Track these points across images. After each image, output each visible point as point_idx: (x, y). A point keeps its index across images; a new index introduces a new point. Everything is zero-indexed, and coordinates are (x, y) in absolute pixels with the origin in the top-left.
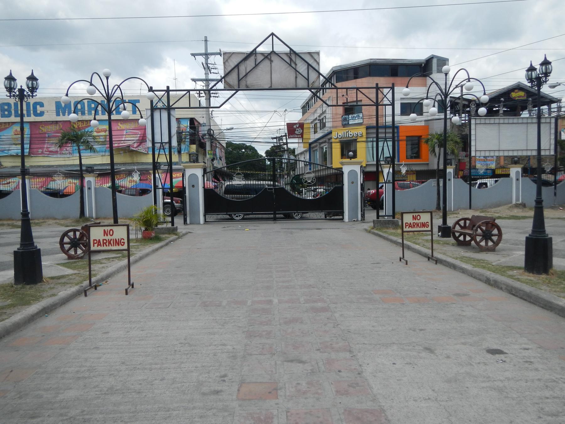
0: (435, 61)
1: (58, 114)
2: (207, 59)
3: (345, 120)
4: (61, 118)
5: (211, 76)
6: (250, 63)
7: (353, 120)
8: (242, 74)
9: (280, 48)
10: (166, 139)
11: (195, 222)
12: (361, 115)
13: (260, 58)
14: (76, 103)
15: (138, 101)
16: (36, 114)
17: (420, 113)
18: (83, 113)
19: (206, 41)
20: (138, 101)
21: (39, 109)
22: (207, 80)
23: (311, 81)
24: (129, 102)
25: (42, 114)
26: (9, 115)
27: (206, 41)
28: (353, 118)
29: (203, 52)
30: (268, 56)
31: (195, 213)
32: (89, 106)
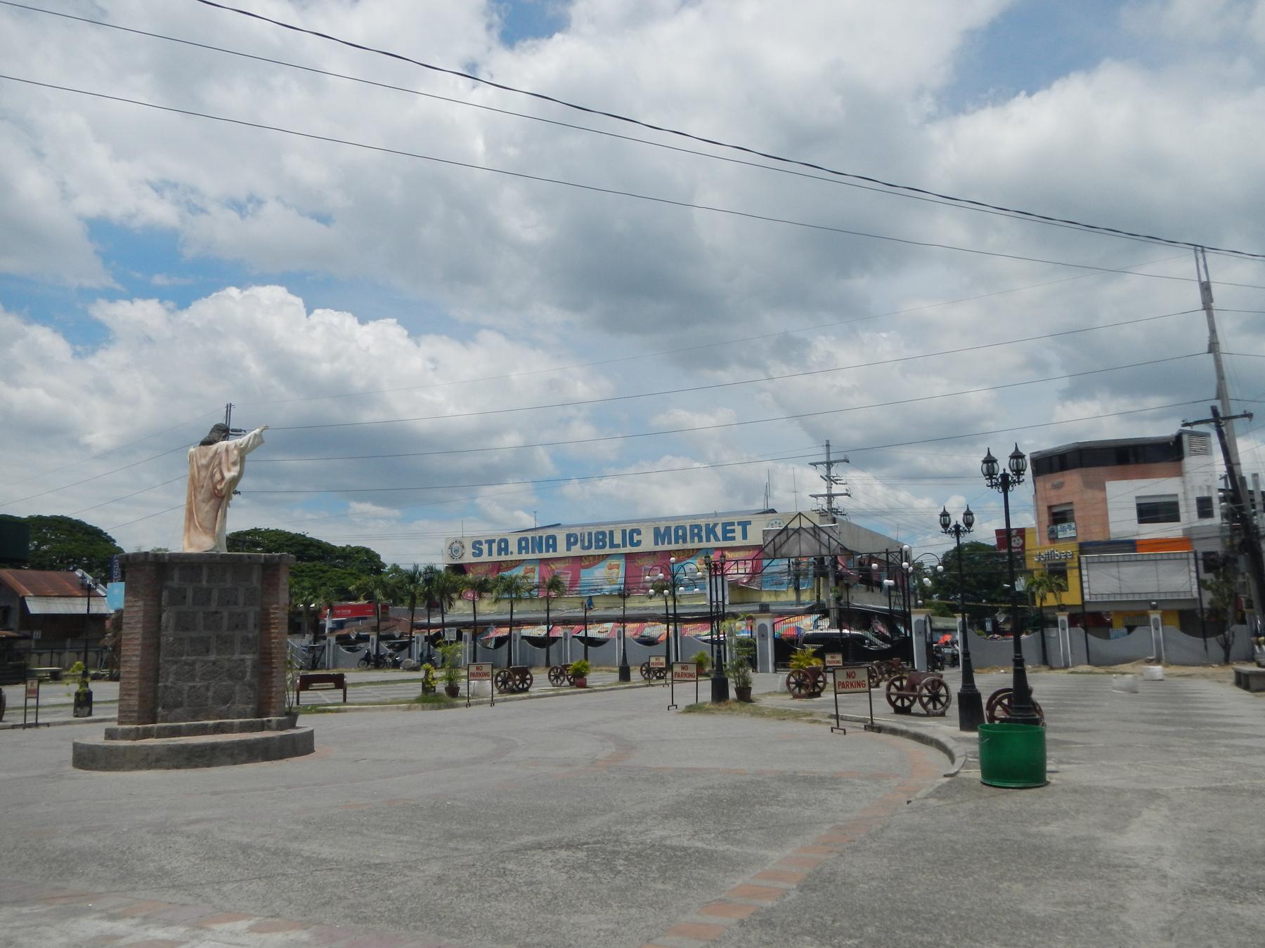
0: (1185, 438)
1: (656, 543)
2: (829, 469)
3: (1052, 532)
4: (660, 548)
5: (836, 489)
6: (783, 537)
7: (1065, 531)
8: (778, 545)
9: (806, 524)
10: (720, 599)
11: (765, 670)
12: (1073, 525)
13: (791, 532)
14: (677, 529)
15: (749, 523)
16: (632, 544)
17: (1176, 518)
18: (685, 541)
19: (828, 446)
20: (749, 523)
21: (636, 538)
22: (830, 497)
23: (832, 548)
24: (739, 523)
25: (639, 543)
26: (604, 546)
27: (828, 446)
28: (1064, 530)
29: (824, 459)
30: (797, 531)
31: (765, 662)
32: (692, 530)
